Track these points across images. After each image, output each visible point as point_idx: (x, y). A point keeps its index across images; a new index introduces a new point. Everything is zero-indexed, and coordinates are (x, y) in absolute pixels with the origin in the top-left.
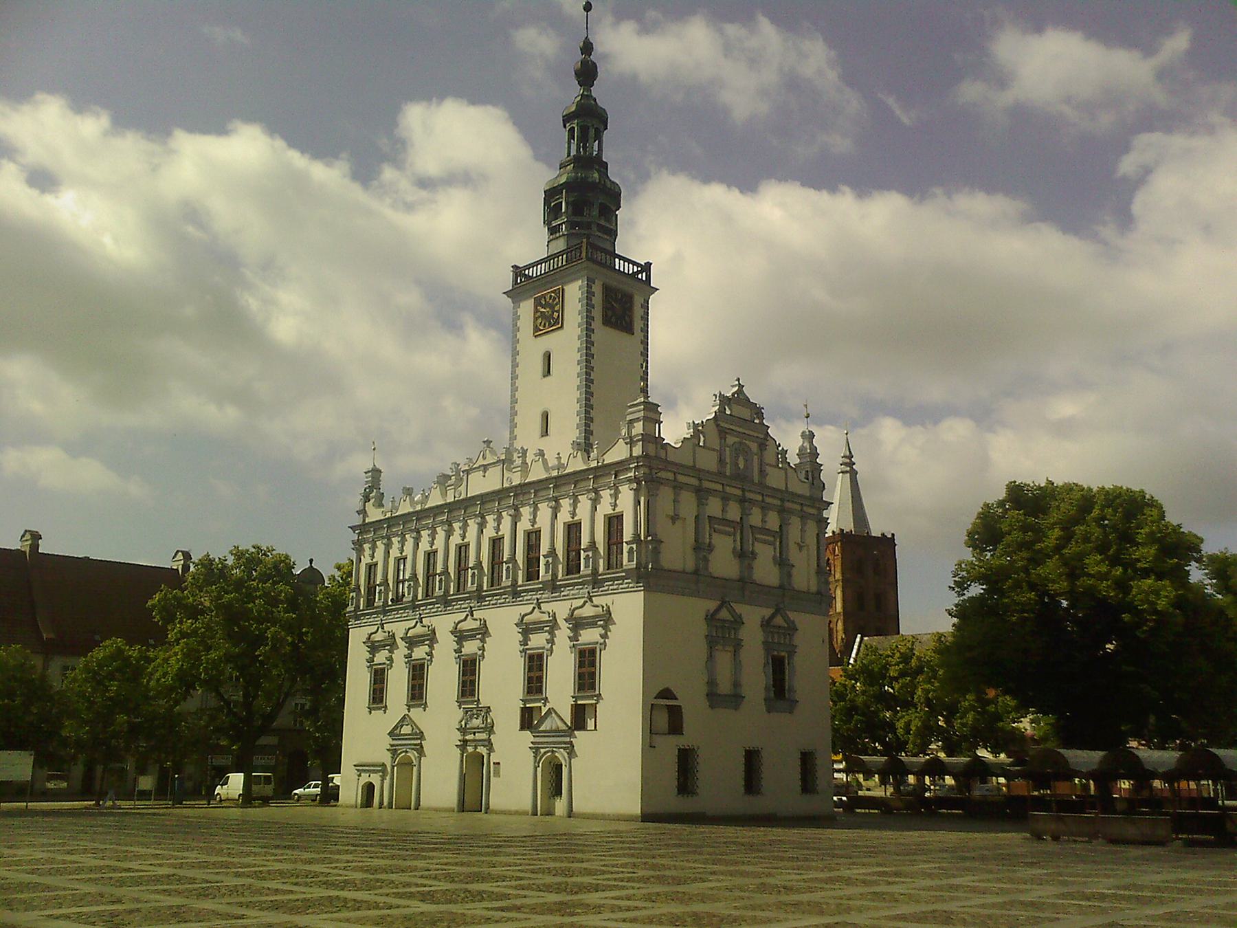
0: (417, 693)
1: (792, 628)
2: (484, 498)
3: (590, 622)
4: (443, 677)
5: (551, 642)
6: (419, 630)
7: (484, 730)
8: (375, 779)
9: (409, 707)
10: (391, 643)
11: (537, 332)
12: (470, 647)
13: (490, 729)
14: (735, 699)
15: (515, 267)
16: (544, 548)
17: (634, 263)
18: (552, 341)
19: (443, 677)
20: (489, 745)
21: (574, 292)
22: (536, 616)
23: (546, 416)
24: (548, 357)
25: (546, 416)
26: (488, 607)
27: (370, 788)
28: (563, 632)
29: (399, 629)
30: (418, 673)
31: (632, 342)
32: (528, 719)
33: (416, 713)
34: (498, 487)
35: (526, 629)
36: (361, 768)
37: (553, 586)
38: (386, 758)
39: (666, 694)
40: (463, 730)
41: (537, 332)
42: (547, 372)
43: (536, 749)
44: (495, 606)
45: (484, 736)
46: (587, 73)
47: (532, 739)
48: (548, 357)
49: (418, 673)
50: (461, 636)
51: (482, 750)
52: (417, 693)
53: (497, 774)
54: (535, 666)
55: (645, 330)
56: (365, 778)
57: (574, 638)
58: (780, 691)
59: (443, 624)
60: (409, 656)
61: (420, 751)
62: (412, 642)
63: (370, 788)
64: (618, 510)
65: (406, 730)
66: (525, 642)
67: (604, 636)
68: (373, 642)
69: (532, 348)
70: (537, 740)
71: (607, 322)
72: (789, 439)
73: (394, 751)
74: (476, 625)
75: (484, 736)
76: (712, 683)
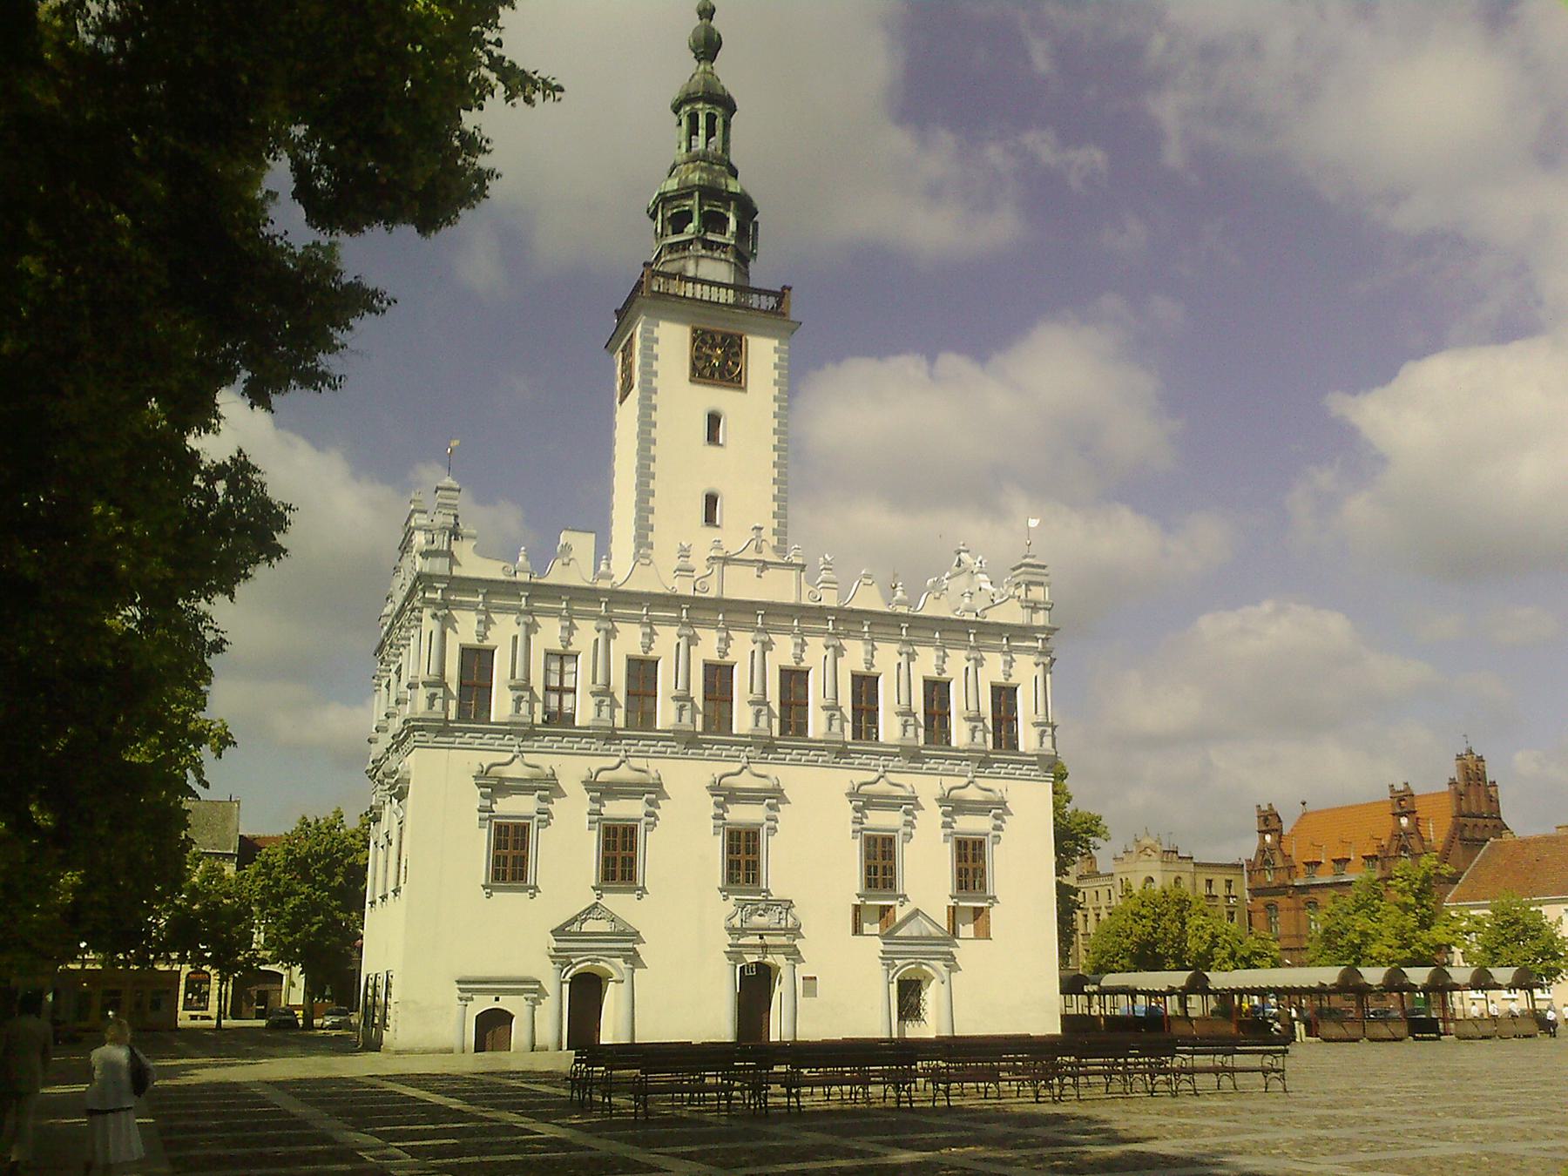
3: (980, 808)
4: (682, 848)
7: (787, 931)
13: (795, 932)
19: (682, 848)
20: (794, 955)
23: (711, 501)
24: (714, 420)
26: (781, 761)
33: (619, 903)
34: (792, 600)
40: (732, 930)
43: (888, 958)
44: (796, 762)
45: (783, 940)
46: (708, 47)
47: (882, 947)
48: (714, 420)
56: (484, 1003)
64: (1012, 681)
67: (998, 828)
70: (888, 948)
75: (783, 940)
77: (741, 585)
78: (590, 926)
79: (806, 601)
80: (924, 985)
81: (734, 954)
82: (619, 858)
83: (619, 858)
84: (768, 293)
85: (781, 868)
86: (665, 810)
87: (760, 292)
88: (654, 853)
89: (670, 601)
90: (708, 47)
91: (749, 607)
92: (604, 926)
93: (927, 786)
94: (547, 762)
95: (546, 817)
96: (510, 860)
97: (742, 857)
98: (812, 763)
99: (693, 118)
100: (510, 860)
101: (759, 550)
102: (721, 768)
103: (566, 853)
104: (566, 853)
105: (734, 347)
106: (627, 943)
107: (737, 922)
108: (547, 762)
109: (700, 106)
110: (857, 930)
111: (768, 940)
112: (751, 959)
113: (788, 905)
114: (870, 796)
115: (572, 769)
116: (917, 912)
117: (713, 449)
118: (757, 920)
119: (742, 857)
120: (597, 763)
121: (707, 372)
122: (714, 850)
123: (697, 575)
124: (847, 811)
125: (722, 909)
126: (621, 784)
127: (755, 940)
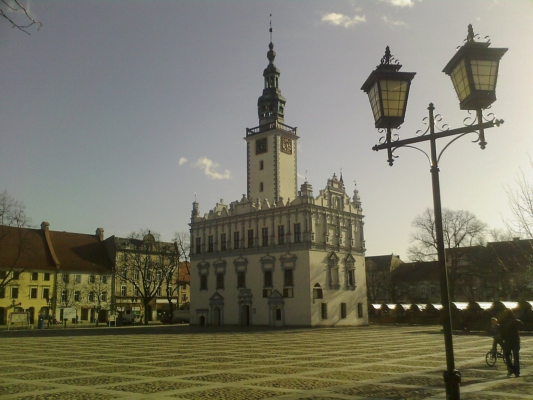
0: (220, 284)
1: (354, 261)
2: (244, 215)
3: (288, 261)
4: (231, 279)
5: (274, 266)
6: (220, 262)
8: (205, 315)
12: (241, 268)
13: (251, 297)
14: (337, 287)
16: (270, 233)
17: (291, 128)
18: (263, 157)
19: (231, 279)
21: (270, 139)
22: (268, 257)
23: (262, 185)
24: (262, 163)
25: (262, 185)
27: (202, 318)
28: (278, 264)
29: (211, 261)
30: (220, 278)
31: (291, 157)
32: (265, 295)
33: (220, 291)
35: (263, 262)
36: (198, 311)
39: (317, 285)
40: (239, 297)
42: (262, 168)
43: (269, 303)
45: (248, 299)
46: (271, 56)
48: (262, 163)
49: (220, 278)
50: (236, 264)
51: (248, 304)
52: (220, 284)
53: (255, 312)
54: (268, 276)
55: (295, 152)
57: (282, 265)
58: (351, 283)
59: (230, 260)
60: (215, 272)
61: (223, 304)
62: (216, 266)
63: (202, 318)
65: (217, 297)
66: (263, 267)
69: (256, 159)
71: (282, 150)
72: (350, 193)
73: (211, 304)
74: (243, 260)
76: (330, 281)
90: (271, 56)
93: (278, 255)
94: (207, 261)
103: (212, 280)
104: (212, 280)
112: (243, 304)
116: (276, 290)
120: (215, 260)
125: (237, 292)
126: (219, 264)
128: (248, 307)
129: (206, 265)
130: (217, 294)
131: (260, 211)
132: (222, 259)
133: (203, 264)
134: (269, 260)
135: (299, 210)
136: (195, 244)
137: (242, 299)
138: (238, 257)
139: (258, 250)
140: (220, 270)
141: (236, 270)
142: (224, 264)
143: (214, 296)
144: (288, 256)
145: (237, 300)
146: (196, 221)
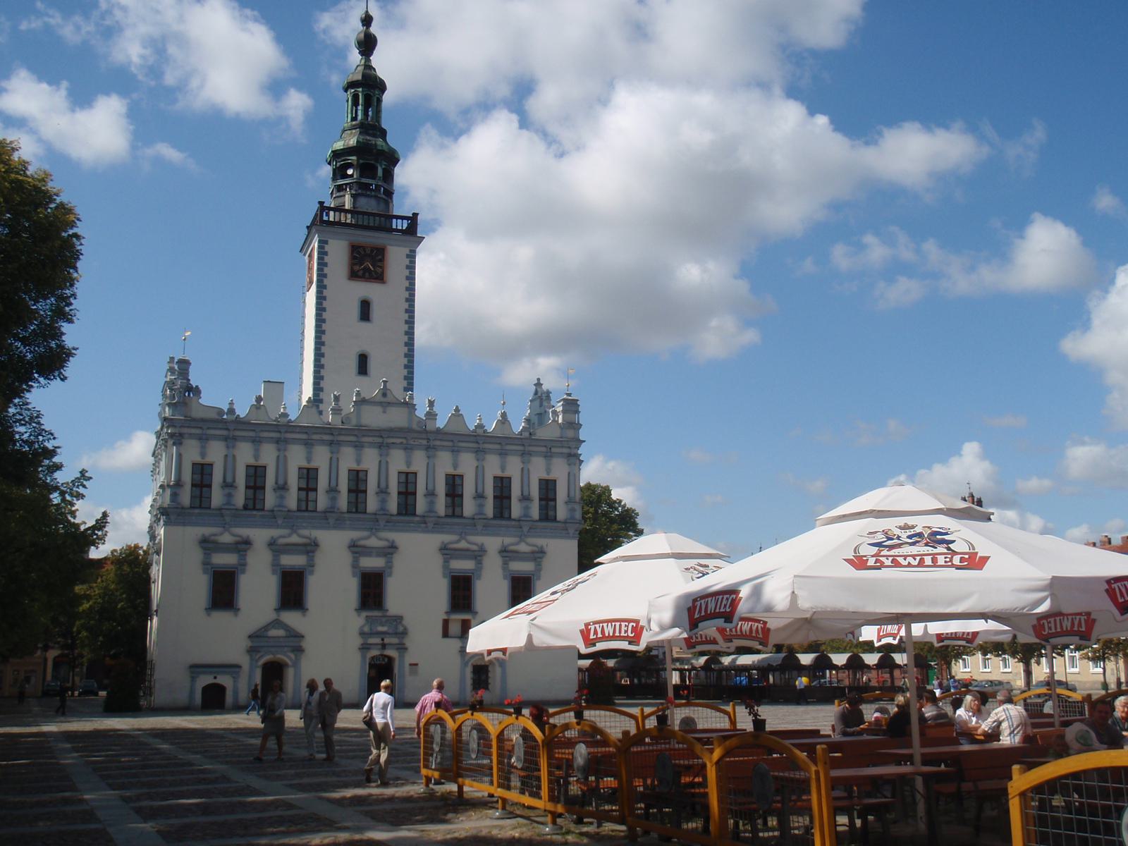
4: (332, 585)
6: (295, 539)
7: (396, 634)
9: (278, 610)
10: (243, 546)
11: (354, 275)
15: (321, 203)
19: (332, 585)
20: (402, 648)
22: (463, 545)
33: (292, 618)
36: (196, 669)
37: (476, 524)
38: (244, 661)
40: (362, 634)
41: (354, 275)
45: (395, 640)
50: (356, 549)
56: (205, 680)
61: (299, 650)
68: (215, 542)
73: (252, 651)
75: (395, 640)
77: (374, 418)
78: (274, 632)
79: (415, 426)
80: (490, 669)
81: (365, 648)
82: (292, 591)
83: (292, 591)
84: (403, 218)
85: (396, 597)
86: (320, 558)
87: (398, 217)
88: (315, 588)
89: (329, 430)
91: (380, 432)
92: (280, 633)
93: (492, 543)
94: (245, 532)
95: (243, 565)
96: (223, 592)
97: (372, 590)
98: (415, 530)
99: (355, 97)
100: (223, 592)
101: (384, 395)
102: (355, 534)
103: (258, 589)
104: (258, 589)
105: (378, 255)
106: (295, 641)
107: (366, 629)
108: (245, 532)
109: (360, 89)
110: (446, 634)
111: (386, 641)
112: (375, 652)
113: (398, 619)
114: (455, 550)
115: (260, 536)
117: (364, 325)
118: (380, 629)
119: (372, 590)
121: (360, 273)
122: (352, 587)
123: (344, 413)
124: (438, 560)
125: (357, 621)
127: (378, 640)
128: (391, 659)
129: (237, 543)
130: (277, 623)
131: (438, 431)
132: (305, 532)
133: (227, 538)
134: (467, 550)
135: (554, 450)
136: (187, 477)
137: (371, 641)
138: (365, 533)
139: (429, 524)
140: (293, 561)
141: (355, 565)
142: (310, 548)
143: (267, 627)
144: (523, 548)
145: (358, 641)
146: (196, 413)
